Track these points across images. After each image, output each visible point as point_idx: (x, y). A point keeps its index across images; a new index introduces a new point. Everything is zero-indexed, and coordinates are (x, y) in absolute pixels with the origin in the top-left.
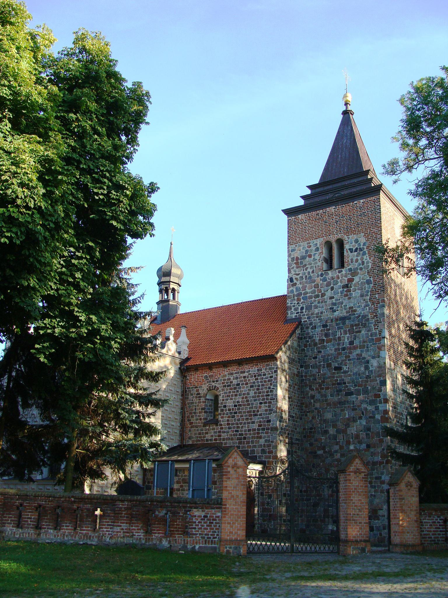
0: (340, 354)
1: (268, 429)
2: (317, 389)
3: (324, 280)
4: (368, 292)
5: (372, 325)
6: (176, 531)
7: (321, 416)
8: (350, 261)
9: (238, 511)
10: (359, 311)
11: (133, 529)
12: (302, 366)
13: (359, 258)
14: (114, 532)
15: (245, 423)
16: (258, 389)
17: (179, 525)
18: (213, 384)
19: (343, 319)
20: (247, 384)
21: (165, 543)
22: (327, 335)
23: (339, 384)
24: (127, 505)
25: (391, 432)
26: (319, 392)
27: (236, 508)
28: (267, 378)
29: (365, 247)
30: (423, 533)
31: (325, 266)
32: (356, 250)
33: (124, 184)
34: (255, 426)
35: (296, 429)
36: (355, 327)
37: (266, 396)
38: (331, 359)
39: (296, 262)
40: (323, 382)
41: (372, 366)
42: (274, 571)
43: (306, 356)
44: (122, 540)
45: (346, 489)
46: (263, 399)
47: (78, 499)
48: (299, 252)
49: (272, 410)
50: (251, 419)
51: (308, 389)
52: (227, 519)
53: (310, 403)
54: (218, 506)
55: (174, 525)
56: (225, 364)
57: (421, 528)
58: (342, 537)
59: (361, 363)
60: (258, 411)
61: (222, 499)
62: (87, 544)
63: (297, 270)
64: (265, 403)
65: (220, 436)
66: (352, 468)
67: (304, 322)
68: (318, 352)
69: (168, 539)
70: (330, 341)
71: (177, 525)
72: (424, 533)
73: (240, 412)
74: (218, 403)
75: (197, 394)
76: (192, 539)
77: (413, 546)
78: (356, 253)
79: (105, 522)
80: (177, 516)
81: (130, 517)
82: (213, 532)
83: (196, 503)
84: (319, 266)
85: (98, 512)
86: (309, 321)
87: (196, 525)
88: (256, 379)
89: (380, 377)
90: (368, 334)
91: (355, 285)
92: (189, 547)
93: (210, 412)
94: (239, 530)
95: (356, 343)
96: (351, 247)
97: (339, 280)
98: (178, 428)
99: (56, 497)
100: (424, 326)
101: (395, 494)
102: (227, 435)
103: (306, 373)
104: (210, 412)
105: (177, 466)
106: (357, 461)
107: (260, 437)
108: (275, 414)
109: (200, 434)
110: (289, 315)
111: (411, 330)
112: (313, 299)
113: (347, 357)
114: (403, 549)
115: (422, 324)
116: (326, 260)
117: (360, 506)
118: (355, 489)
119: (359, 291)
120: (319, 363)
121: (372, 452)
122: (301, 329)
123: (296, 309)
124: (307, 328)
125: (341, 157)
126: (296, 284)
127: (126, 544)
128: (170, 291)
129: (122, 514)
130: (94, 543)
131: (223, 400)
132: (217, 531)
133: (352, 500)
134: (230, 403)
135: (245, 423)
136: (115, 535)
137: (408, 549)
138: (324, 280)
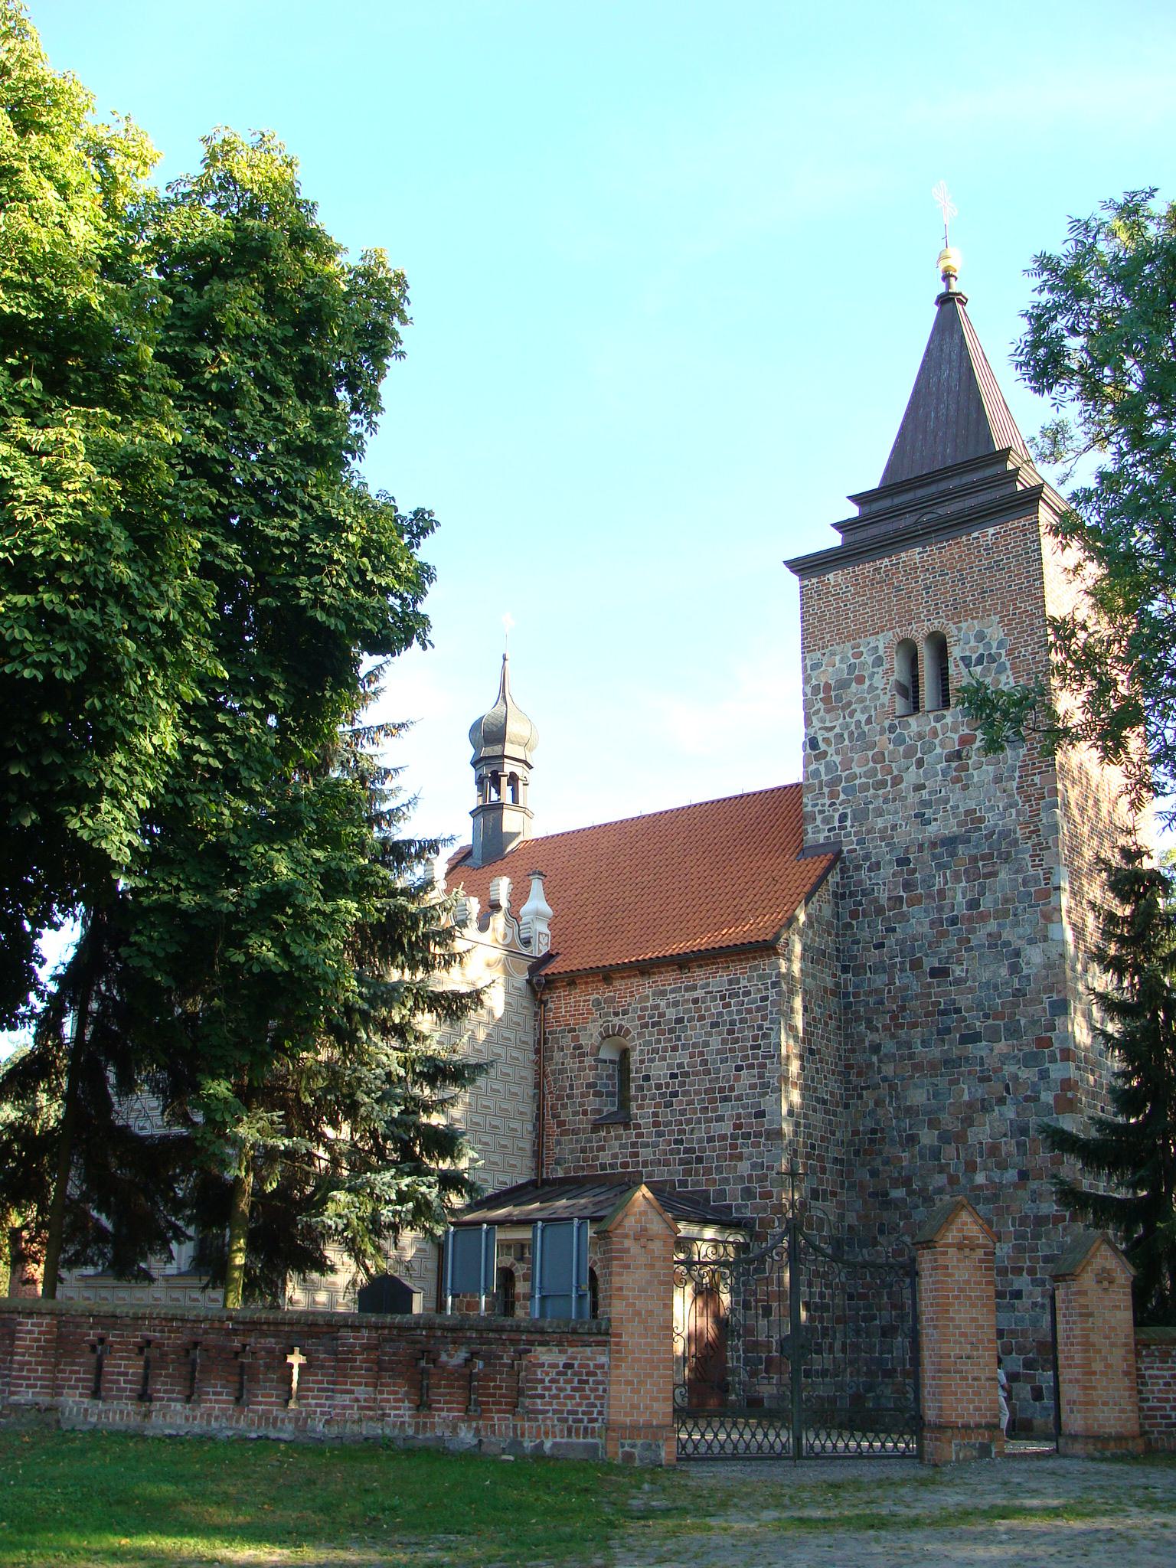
0: (943, 934)
1: (758, 1135)
2: (886, 1028)
3: (899, 741)
5: (1027, 856)
6: (494, 1403)
7: (897, 1099)
9: (653, 1352)
10: (991, 820)
11: (382, 1400)
12: (845, 969)
14: (334, 1407)
16: (731, 1032)
17: (501, 1388)
18: (616, 1021)
19: (950, 842)
20: (701, 1018)
21: (466, 1435)
22: (908, 886)
23: (943, 1013)
25: (1062, 1141)
26: (893, 1036)
27: (646, 1344)
29: (1003, 652)
30: (1145, 1405)
31: (900, 705)
33: (341, 518)
34: (726, 1128)
36: (980, 864)
37: (753, 1048)
38: (921, 947)
39: (824, 697)
40: (903, 1008)
41: (1028, 964)
42: (735, 1505)
43: (858, 942)
44: (356, 1428)
45: (936, 1290)
47: (244, 1323)
48: (830, 669)
50: (715, 1110)
53: (870, 1065)
54: (600, 1338)
56: (644, 969)
57: (1140, 1392)
58: (930, 1415)
60: (732, 1089)
61: (609, 1320)
62: (268, 1438)
63: (828, 717)
64: (751, 1067)
65: (636, 1155)
66: (952, 1236)
67: (849, 851)
69: (474, 1424)
70: (918, 900)
71: (495, 1387)
72: (1151, 1404)
73: (686, 1093)
74: (629, 1071)
77: (1120, 1438)
78: (979, 668)
79: (314, 1382)
80: (495, 1365)
82: (587, 1405)
83: (542, 1332)
84: (883, 705)
86: (862, 849)
88: (728, 1005)
89: (1051, 991)
90: (1015, 880)
92: (528, 1444)
93: (609, 1094)
94: (656, 1399)
95: (986, 904)
96: (967, 654)
97: (937, 741)
98: (529, 1136)
99: (187, 1320)
100: (1145, 858)
101: (1070, 1301)
103: (856, 986)
104: (609, 1094)
105: (500, 1235)
106: (965, 1217)
109: (583, 1150)
110: (810, 835)
112: (872, 791)
114: (1091, 1447)
115: (1132, 855)
117: (975, 1335)
118: (961, 1290)
119: (991, 768)
120: (891, 958)
121: (1034, 1192)
123: (827, 820)
124: (858, 868)
125: (937, 418)
126: (825, 753)
127: (366, 1439)
128: (504, 780)
129: (355, 1360)
130: (284, 1436)
131: (642, 1062)
132: (598, 1402)
133: (952, 1319)
134: (659, 1071)
136: (337, 1415)
137: (1106, 1447)
138: (899, 741)
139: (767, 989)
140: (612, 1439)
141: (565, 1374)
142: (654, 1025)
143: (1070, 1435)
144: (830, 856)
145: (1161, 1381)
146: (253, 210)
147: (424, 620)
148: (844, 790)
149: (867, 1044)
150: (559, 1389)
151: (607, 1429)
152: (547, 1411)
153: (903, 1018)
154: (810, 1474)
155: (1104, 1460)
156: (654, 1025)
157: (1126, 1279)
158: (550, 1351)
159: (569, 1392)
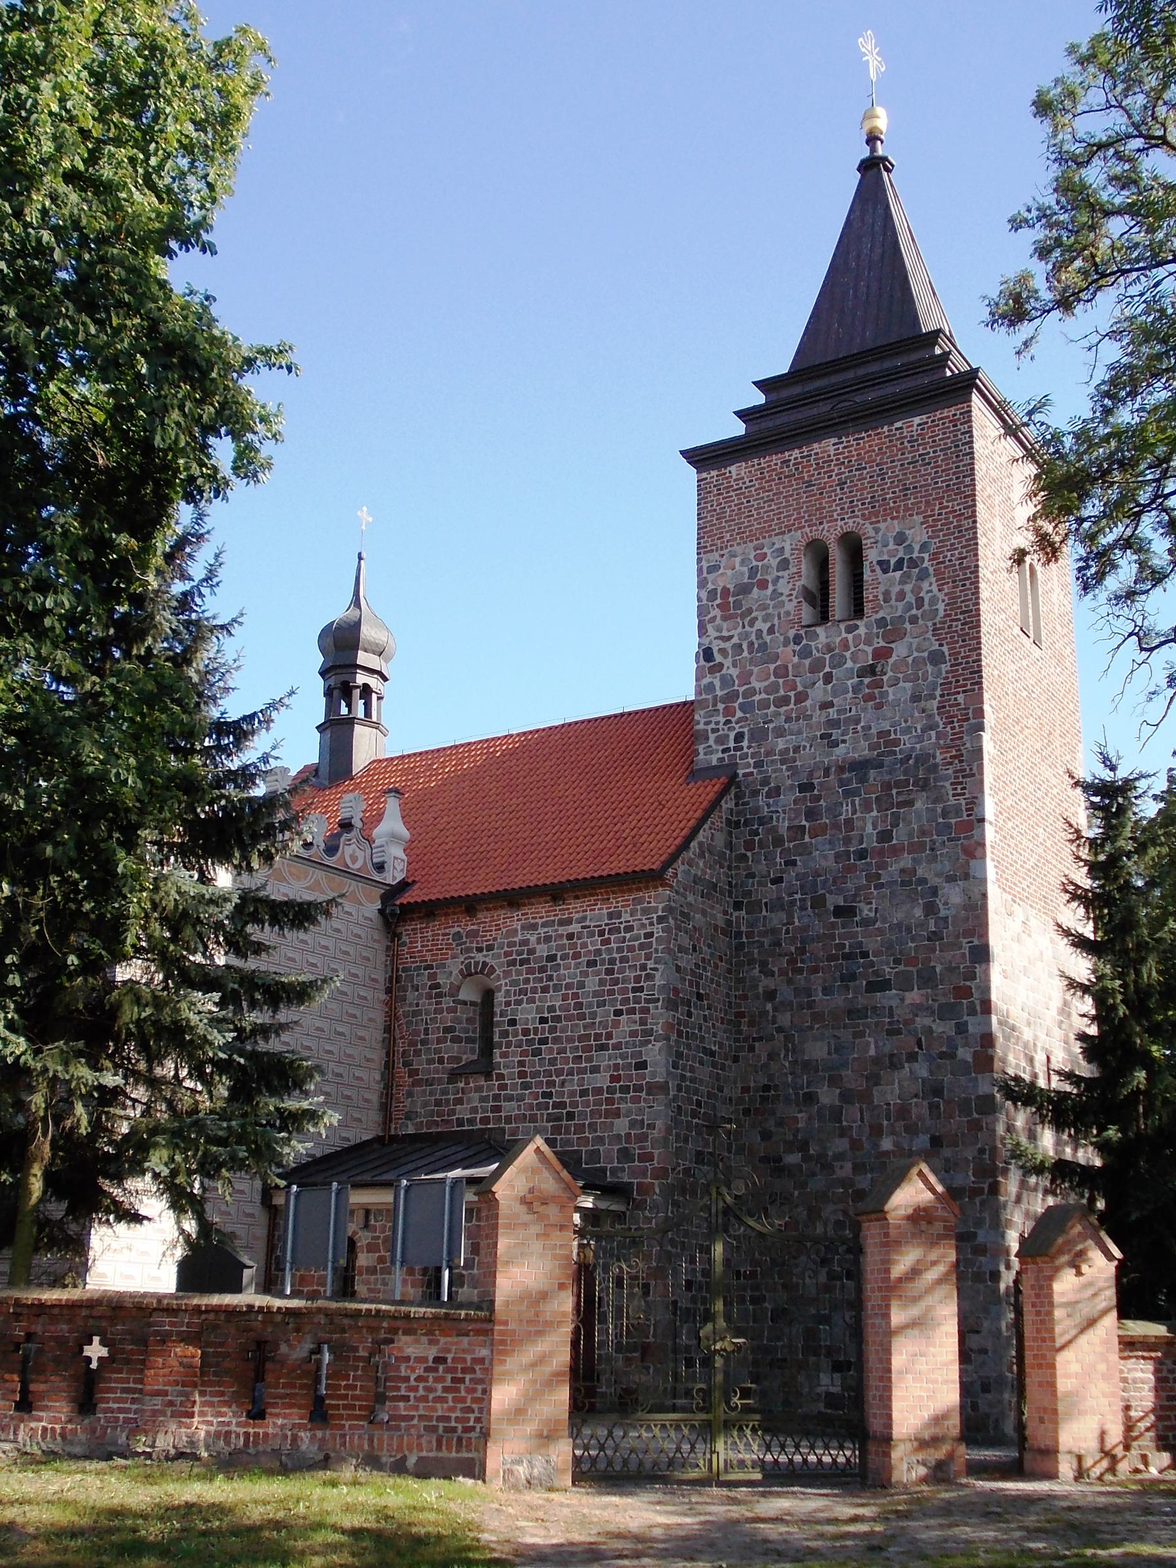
0: (850, 869)
1: (638, 1088)
3: (805, 653)
5: (947, 784)
6: (345, 1407)
7: (794, 1051)
8: (881, 597)
10: (907, 742)
12: (738, 906)
13: (908, 588)
16: (609, 972)
18: (480, 957)
19: (860, 767)
20: (577, 956)
22: (811, 814)
23: (846, 957)
26: (790, 982)
28: (637, 938)
31: (807, 614)
32: (899, 565)
34: (602, 1080)
35: (721, 1090)
36: (894, 791)
37: (635, 990)
38: (825, 882)
39: (720, 603)
40: (802, 951)
43: (751, 875)
46: (626, 1001)
48: (729, 572)
51: (756, 972)
55: (338, 1387)
56: (513, 899)
60: (609, 1036)
63: (725, 625)
64: (632, 1011)
65: (497, 1109)
67: (745, 775)
68: (787, 863)
70: (823, 830)
71: (347, 1387)
73: (556, 1040)
74: (492, 1014)
78: (898, 574)
79: (117, 1381)
84: (788, 613)
85: (96, 1351)
86: (760, 772)
87: (410, 1389)
90: (934, 810)
93: (469, 1040)
95: (900, 836)
96: (885, 557)
97: (848, 654)
98: (376, 1086)
104: (469, 1040)
107: (617, 1114)
108: (659, 1044)
109: (438, 1103)
110: (701, 756)
112: (772, 708)
113: (873, 877)
116: (808, 596)
119: (909, 685)
120: (790, 895)
121: (947, 1160)
122: (737, 797)
123: (721, 740)
124: (755, 793)
125: (856, 297)
126: (721, 665)
131: (508, 1004)
134: (527, 1014)
138: (805, 653)
139: (652, 924)
142: (522, 962)
144: (723, 779)
148: (742, 707)
149: (761, 990)
150: (429, 1389)
152: (413, 1417)
153: (803, 962)
156: (522, 962)
158: (417, 1342)
159: (439, 1393)
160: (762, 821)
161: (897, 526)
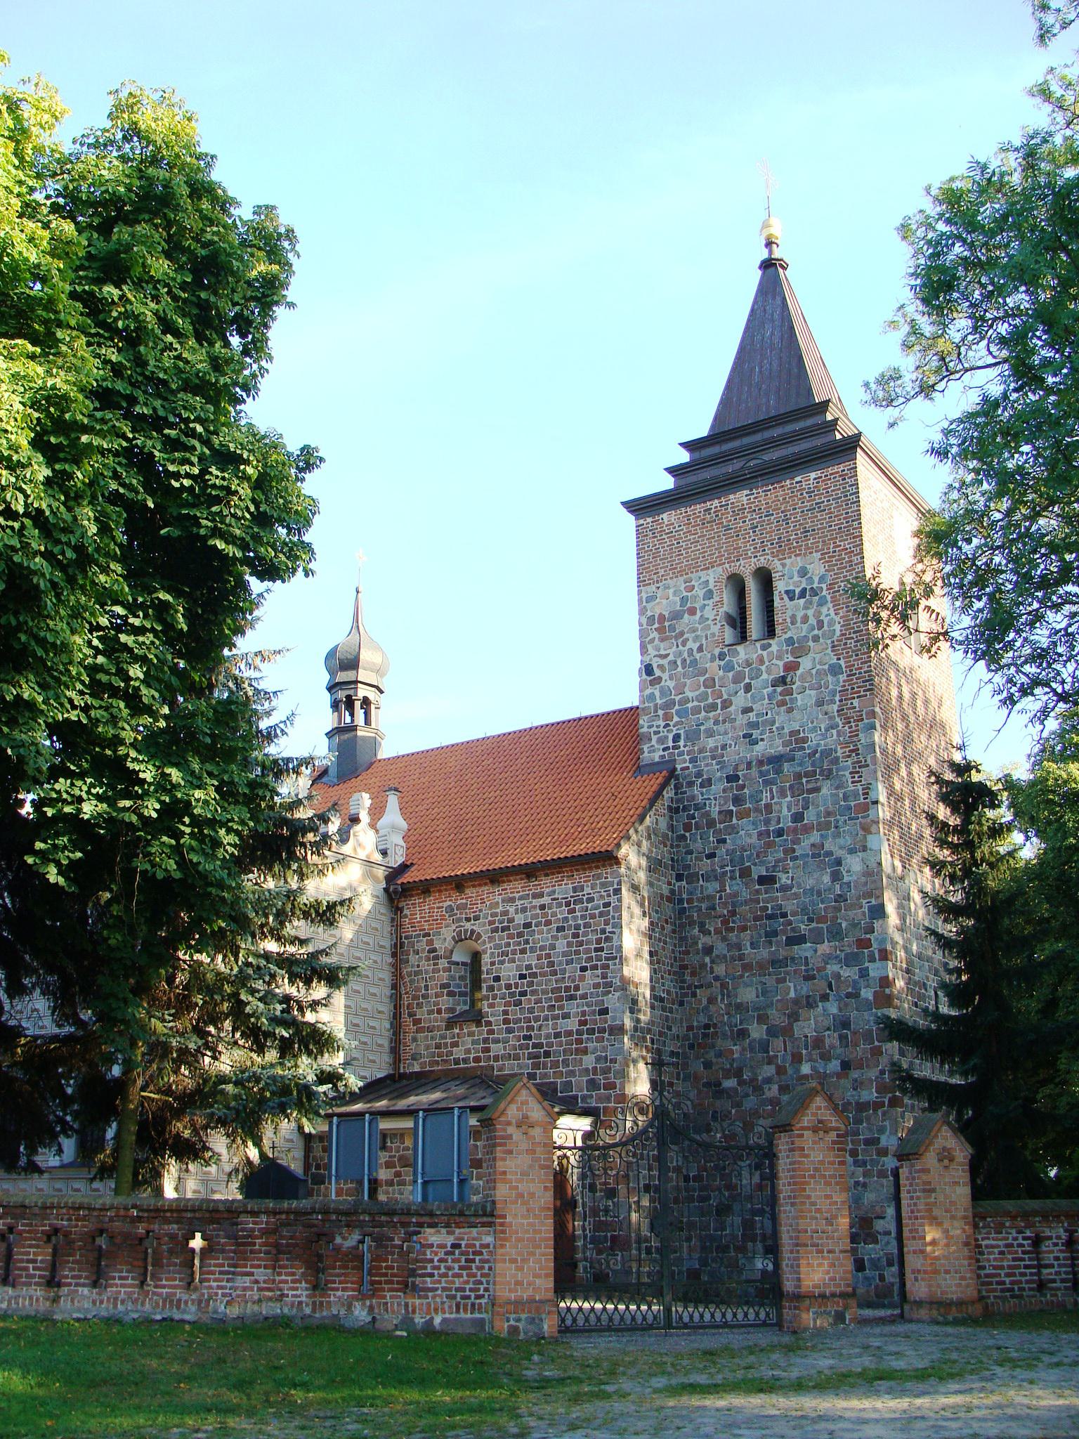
0: (769, 845)
1: (602, 1030)
2: (717, 931)
3: (729, 668)
4: (833, 693)
5: (847, 773)
6: (386, 1282)
7: (729, 996)
8: (789, 620)
9: (535, 1231)
10: (814, 740)
11: (281, 1282)
12: (679, 877)
13: (810, 613)
14: (236, 1289)
15: (546, 1019)
16: (576, 935)
18: (468, 926)
19: (776, 761)
20: (548, 923)
21: (360, 1314)
22: (737, 800)
23: (769, 917)
24: (267, 1223)
25: (897, 1030)
26: (724, 939)
27: (529, 1224)
29: (824, 586)
30: (982, 1272)
31: (729, 635)
32: (803, 594)
33: (238, 452)
35: (670, 1028)
36: (804, 780)
37: (596, 950)
38: (749, 857)
39: (659, 627)
40: (733, 913)
41: (848, 871)
42: (624, 1374)
43: (691, 852)
44: (256, 1308)
45: (794, 1170)
47: (148, 1211)
48: (664, 601)
49: (610, 985)
51: (696, 931)
52: (509, 1250)
53: (703, 966)
54: (485, 1219)
56: (494, 877)
57: (978, 1261)
58: (788, 1286)
59: (821, 867)
60: (577, 988)
61: (494, 1202)
62: (172, 1320)
63: (662, 645)
64: (595, 967)
65: (487, 1050)
66: (806, 1120)
67: (682, 769)
69: (368, 1303)
71: (386, 1268)
72: (987, 1271)
73: (534, 992)
74: (480, 972)
75: (429, 952)
76: (425, 1301)
77: (960, 1303)
78: (802, 601)
79: (216, 1265)
80: (387, 1247)
81: (274, 1251)
82: (474, 1283)
83: (431, 1214)
84: (713, 635)
85: (197, 1243)
86: (695, 767)
87: (435, 1268)
91: (802, 679)
92: (419, 1320)
93: (462, 994)
94: (539, 1276)
95: (810, 816)
96: (791, 588)
97: (763, 668)
99: (94, 1209)
100: (973, 772)
101: (914, 1178)
102: (505, 1048)
103: (690, 893)
104: (462, 994)
105: (385, 1124)
106: (819, 1101)
107: (585, 1051)
108: (617, 994)
109: (438, 1046)
110: (646, 754)
111: (939, 781)
112: (703, 713)
114: (935, 1313)
115: (964, 769)
116: (731, 621)
118: (816, 1169)
119: (813, 693)
120: (722, 867)
121: (855, 1080)
123: (662, 740)
124: (691, 784)
125: (760, 372)
126: (660, 678)
127: (266, 1318)
128: (357, 704)
129: (254, 1244)
130: (187, 1317)
131: (493, 964)
132: (484, 1280)
133: (809, 1197)
134: (509, 972)
135: (546, 1019)
136: (238, 1296)
138: (729, 668)
139: (609, 896)
140: (498, 1313)
141: (453, 1253)
143: (915, 1302)
145: (996, 1250)
146: (155, 161)
147: (308, 548)
148: (678, 713)
150: (448, 1268)
151: (493, 1305)
152: (437, 1289)
154: (683, 1342)
155: (946, 1323)
157: (965, 1157)
159: (456, 1271)
160: (697, 807)
161: (800, 562)
